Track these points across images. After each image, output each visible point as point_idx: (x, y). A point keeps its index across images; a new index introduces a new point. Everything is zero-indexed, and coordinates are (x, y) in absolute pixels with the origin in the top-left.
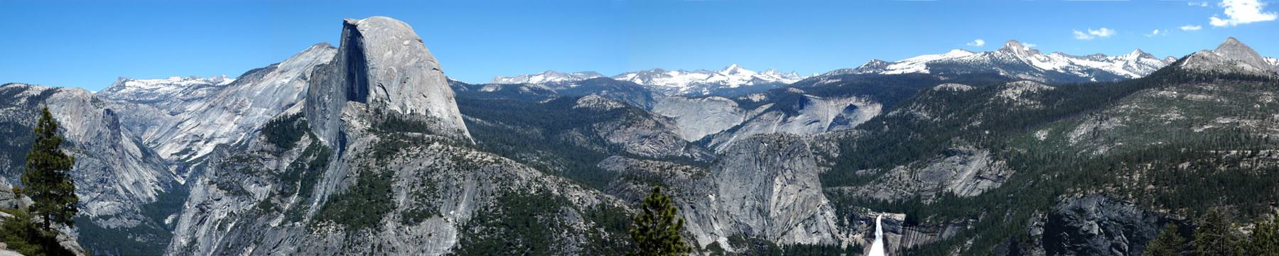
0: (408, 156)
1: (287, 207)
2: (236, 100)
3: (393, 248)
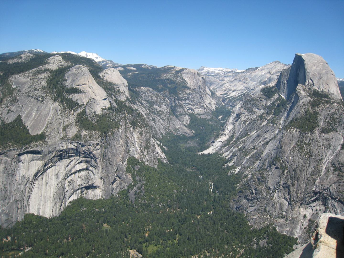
0: (324, 107)
1: (269, 118)
2: (245, 78)
3: (318, 141)
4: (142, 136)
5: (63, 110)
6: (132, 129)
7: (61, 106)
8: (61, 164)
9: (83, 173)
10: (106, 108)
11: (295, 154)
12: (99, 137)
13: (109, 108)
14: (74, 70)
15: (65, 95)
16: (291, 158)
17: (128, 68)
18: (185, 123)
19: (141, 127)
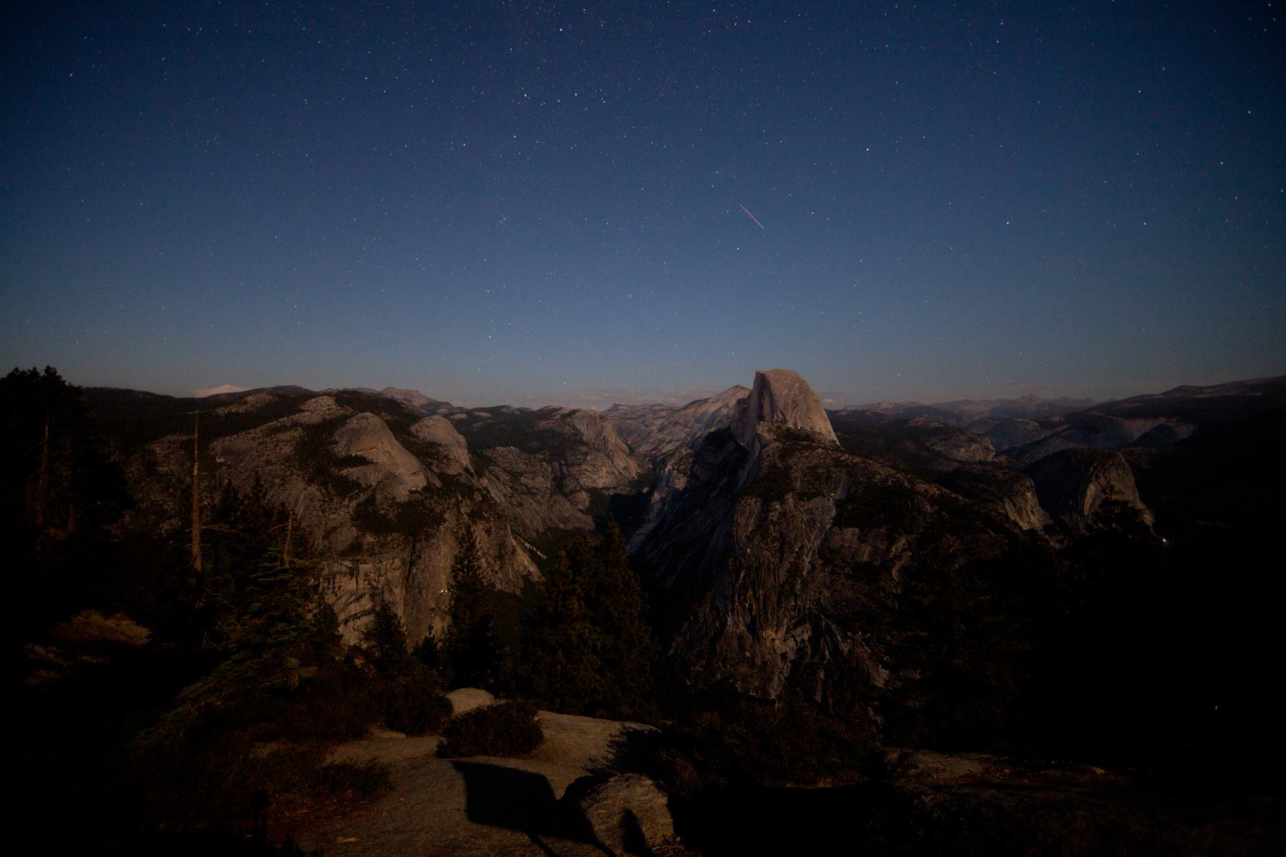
1: (721, 484)
4: (489, 536)
5: (327, 499)
10: (418, 489)
11: (756, 541)
13: (425, 489)
14: (353, 423)
16: (749, 550)
17: (476, 414)
18: (581, 507)
19: (487, 520)
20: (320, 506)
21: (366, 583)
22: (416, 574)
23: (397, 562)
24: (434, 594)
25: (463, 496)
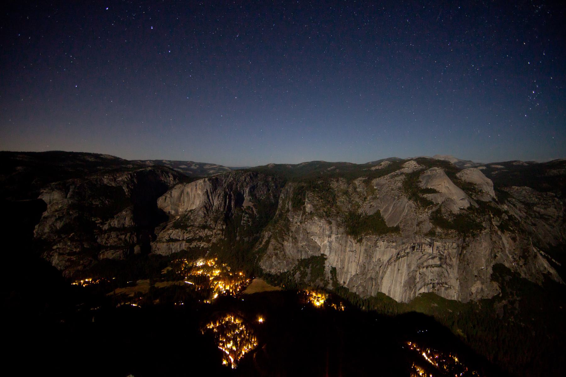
5: (417, 208)
6: (499, 233)
7: (416, 204)
8: (413, 256)
9: (436, 269)
10: (465, 208)
12: (455, 236)
13: (468, 208)
14: (429, 172)
15: (419, 194)
17: (493, 166)
19: (513, 232)
20: (415, 211)
21: (437, 251)
22: (465, 254)
23: (455, 245)
24: (477, 268)
25: (493, 215)
